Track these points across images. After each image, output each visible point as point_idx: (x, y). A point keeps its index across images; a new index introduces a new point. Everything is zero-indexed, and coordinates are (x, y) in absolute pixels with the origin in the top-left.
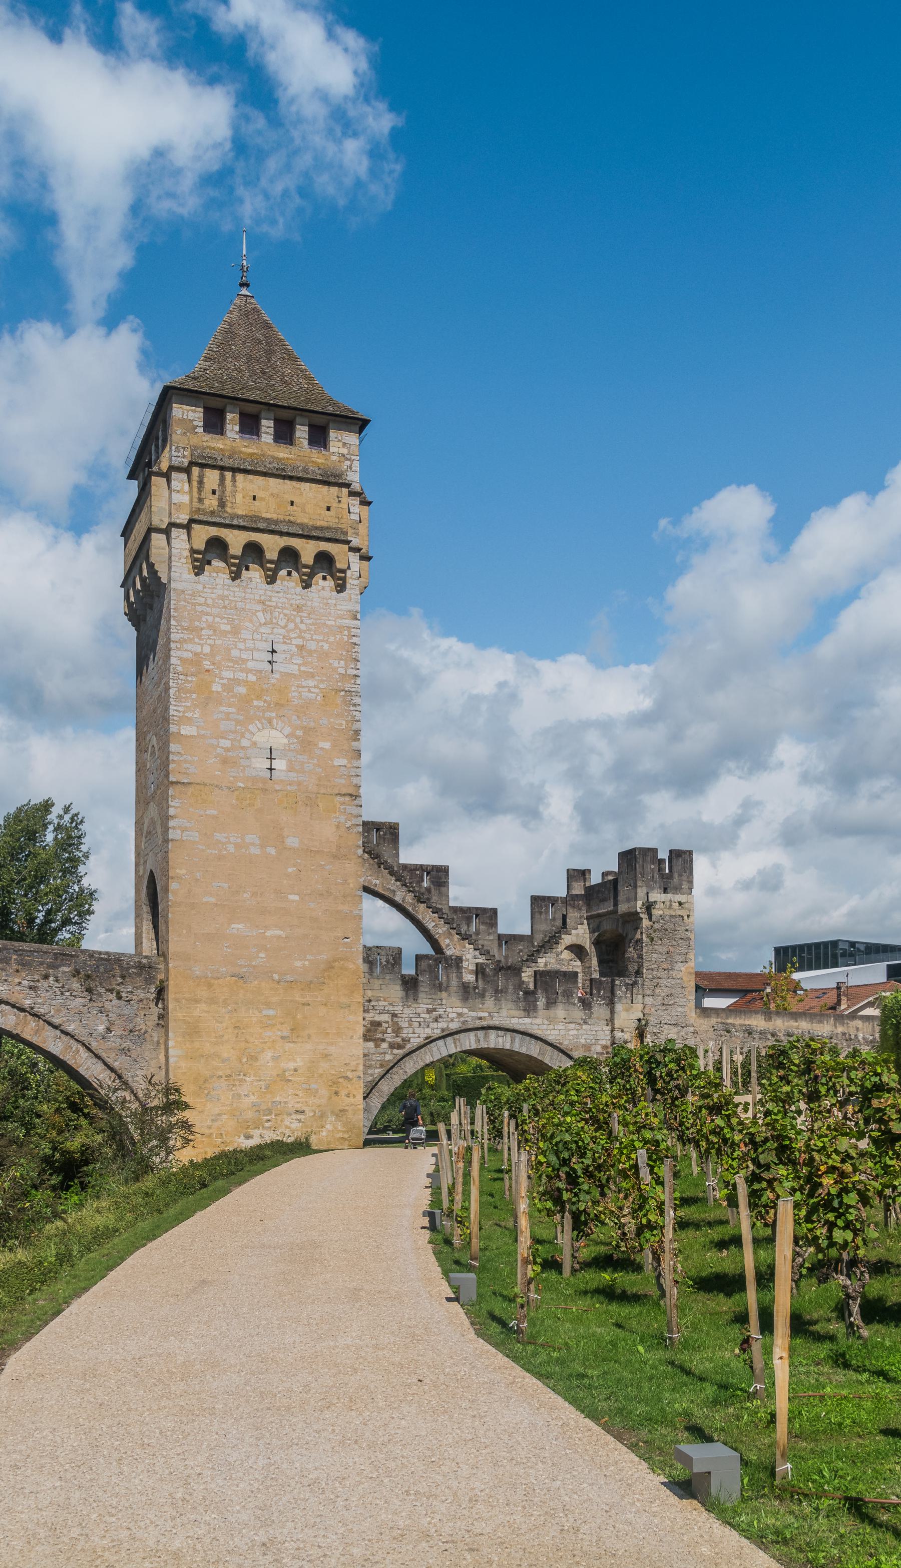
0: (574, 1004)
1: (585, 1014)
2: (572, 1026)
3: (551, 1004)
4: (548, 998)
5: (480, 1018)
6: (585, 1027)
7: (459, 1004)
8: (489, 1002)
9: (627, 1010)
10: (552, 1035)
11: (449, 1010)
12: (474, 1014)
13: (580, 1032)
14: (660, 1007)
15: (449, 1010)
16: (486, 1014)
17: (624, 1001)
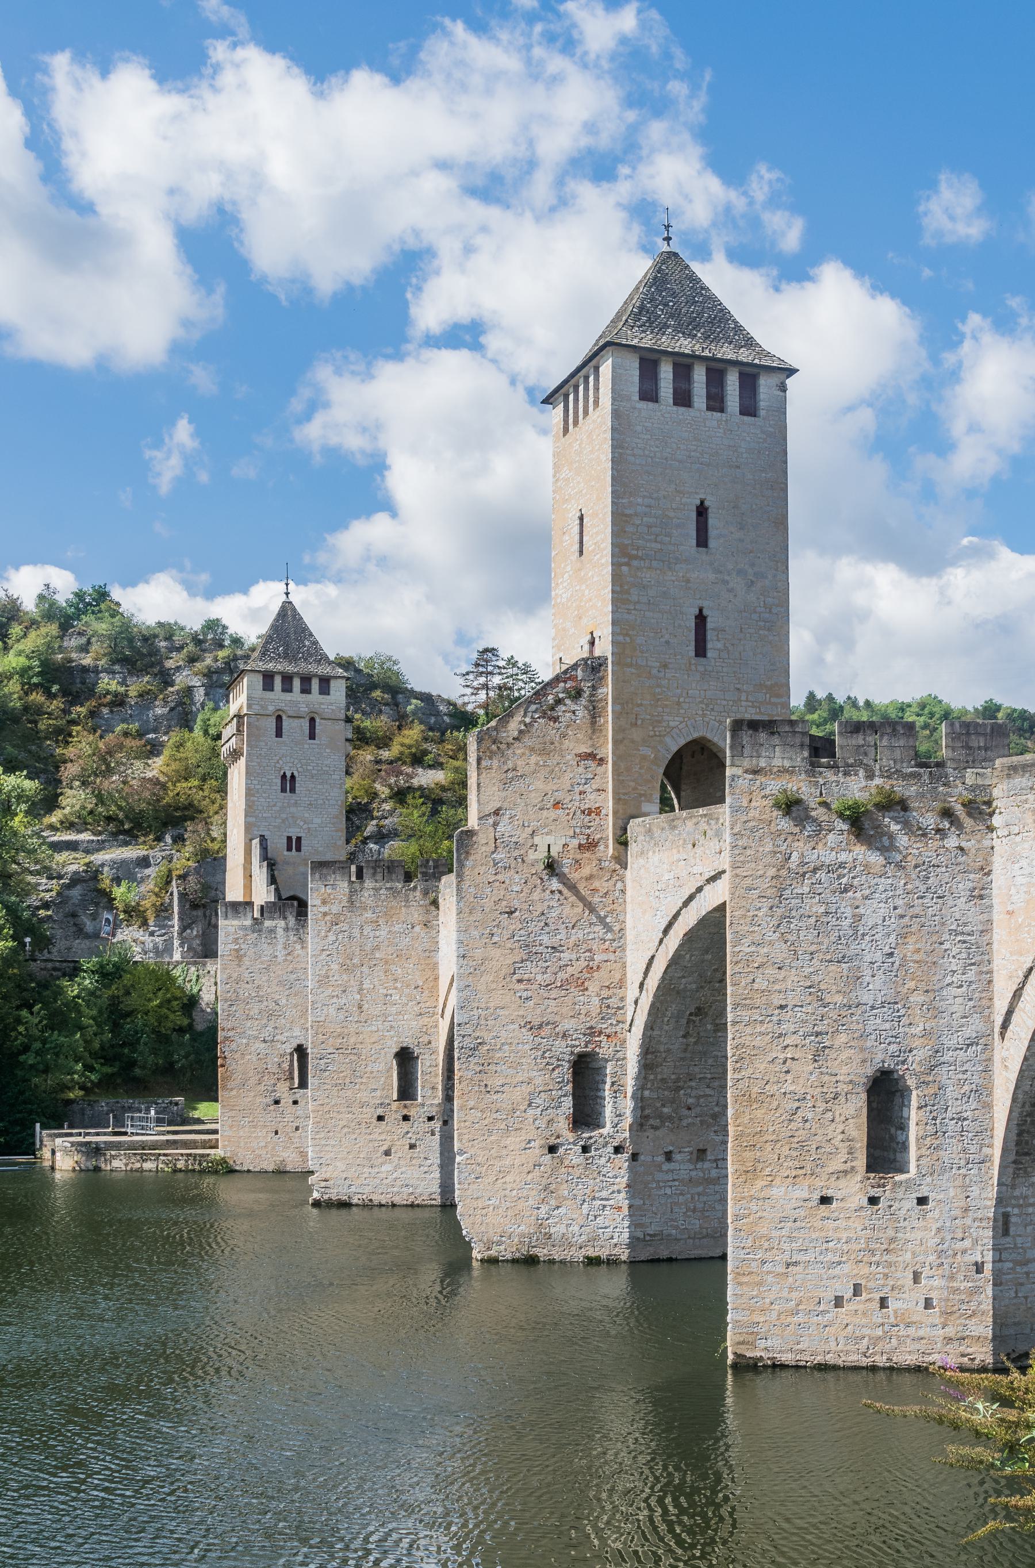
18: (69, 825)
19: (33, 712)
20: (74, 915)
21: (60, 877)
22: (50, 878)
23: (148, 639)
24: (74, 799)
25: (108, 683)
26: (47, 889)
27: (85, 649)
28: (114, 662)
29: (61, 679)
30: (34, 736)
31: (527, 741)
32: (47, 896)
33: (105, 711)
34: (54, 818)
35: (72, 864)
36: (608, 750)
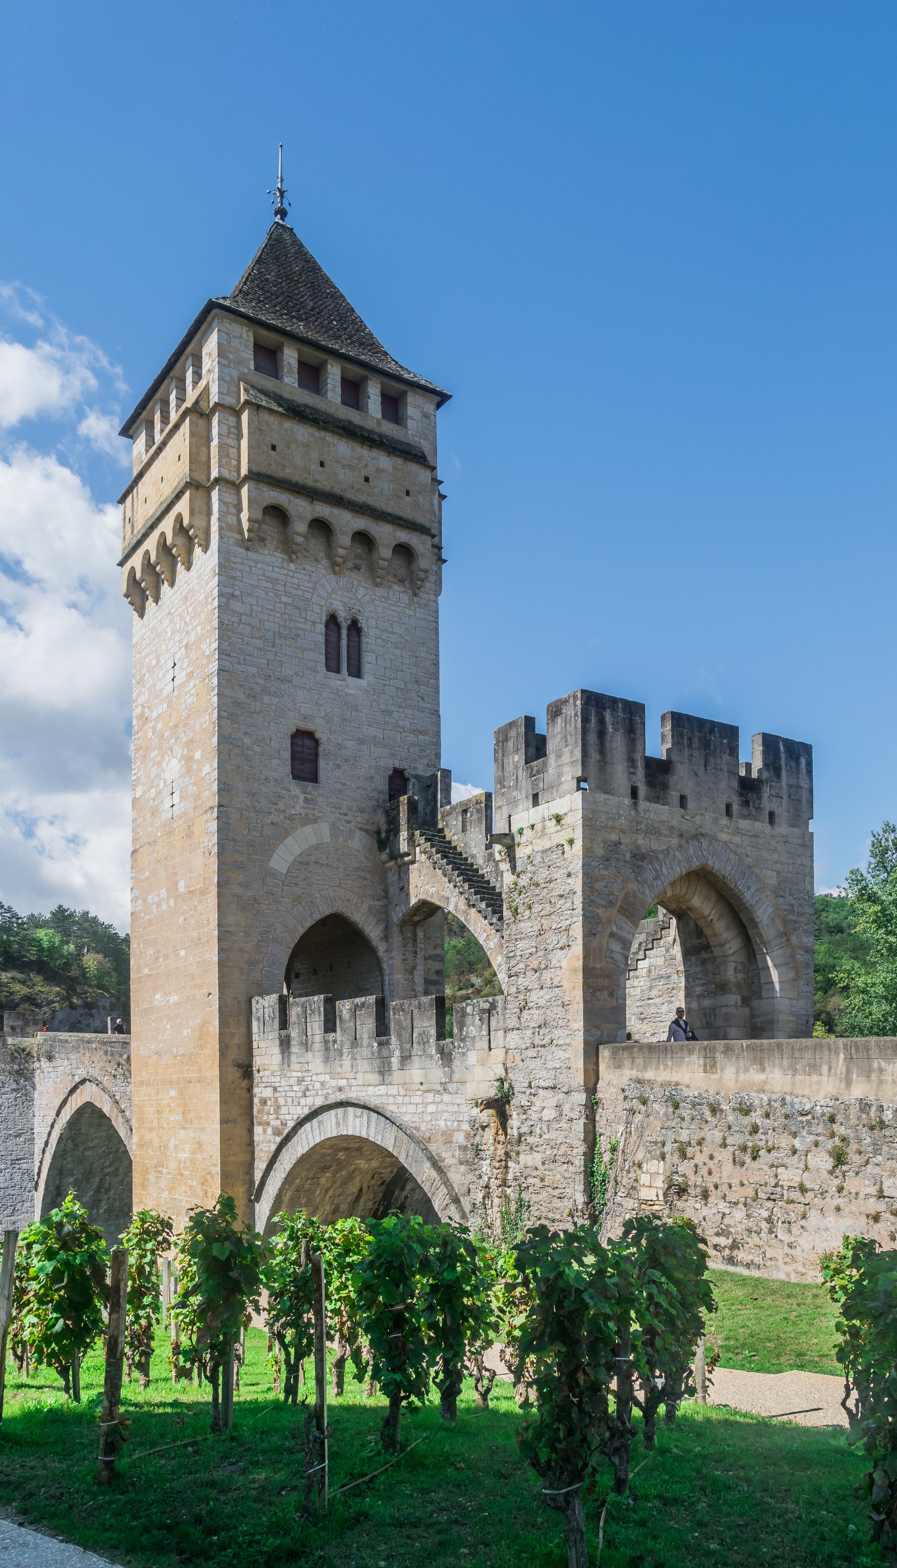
0: (431, 1057)
1: (444, 1072)
2: (430, 1097)
3: (406, 1059)
4: (402, 1049)
5: (340, 1089)
6: (446, 1098)
7: (321, 1070)
8: (347, 1062)
9: (482, 1063)
10: (407, 1114)
11: (315, 1078)
12: (334, 1083)
13: (441, 1107)
14: (531, 1053)
15: (315, 1078)
16: (343, 1083)
17: (478, 1045)
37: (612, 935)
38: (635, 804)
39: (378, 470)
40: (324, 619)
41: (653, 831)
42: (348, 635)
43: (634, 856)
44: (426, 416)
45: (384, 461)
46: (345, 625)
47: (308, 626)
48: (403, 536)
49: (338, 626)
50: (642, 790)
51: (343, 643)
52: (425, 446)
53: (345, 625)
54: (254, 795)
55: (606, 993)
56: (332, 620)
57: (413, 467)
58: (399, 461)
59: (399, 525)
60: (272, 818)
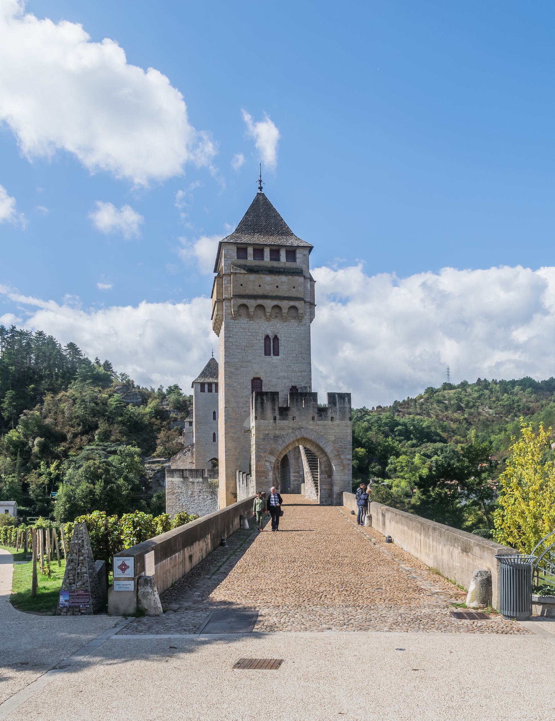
18: (159, 456)
19: (151, 424)
20: (158, 481)
21: (154, 470)
22: (152, 471)
23: (184, 401)
24: (160, 449)
25: (173, 415)
26: (150, 474)
27: (168, 405)
28: (175, 409)
29: (160, 414)
30: (152, 431)
31: (181, 460)
32: (151, 476)
33: (172, 423)
34: (155, 454)
35: (157, 467)
36: (194, 461)
37: (266, 461)
38: (275, 422)
39: (282, 282)
40: (264, 338)
41: (282, 429)
42: (273, 342)
43: (275, 437)
44: (305, 255)
45: (284, 278)
46: (272, 338)
47: (257, 342)
48: (292, 303)
49: (270, 339)
50: (278, 417)
51: (272, 345)
52: (304, 267)
53: (272, 338)
54: (238, 402)
55: (264, 478)
56: (267, 338)
57: (296, 278)
58: (290, 277)
59: (291, 300)
60: (244, 409)
